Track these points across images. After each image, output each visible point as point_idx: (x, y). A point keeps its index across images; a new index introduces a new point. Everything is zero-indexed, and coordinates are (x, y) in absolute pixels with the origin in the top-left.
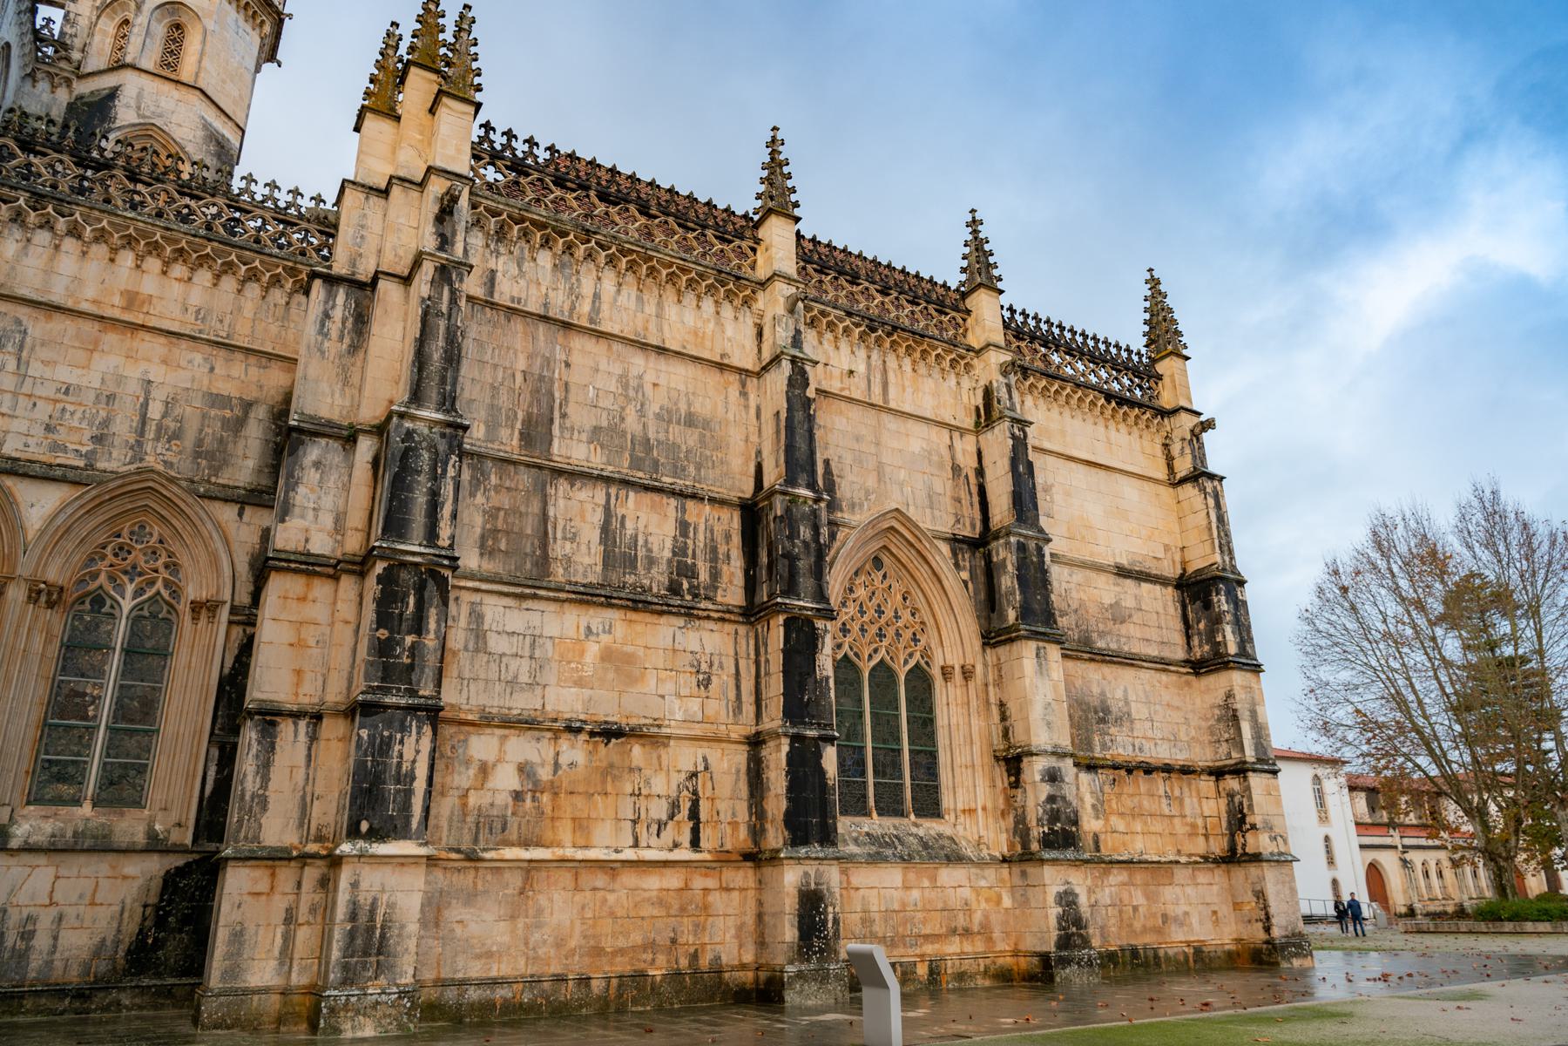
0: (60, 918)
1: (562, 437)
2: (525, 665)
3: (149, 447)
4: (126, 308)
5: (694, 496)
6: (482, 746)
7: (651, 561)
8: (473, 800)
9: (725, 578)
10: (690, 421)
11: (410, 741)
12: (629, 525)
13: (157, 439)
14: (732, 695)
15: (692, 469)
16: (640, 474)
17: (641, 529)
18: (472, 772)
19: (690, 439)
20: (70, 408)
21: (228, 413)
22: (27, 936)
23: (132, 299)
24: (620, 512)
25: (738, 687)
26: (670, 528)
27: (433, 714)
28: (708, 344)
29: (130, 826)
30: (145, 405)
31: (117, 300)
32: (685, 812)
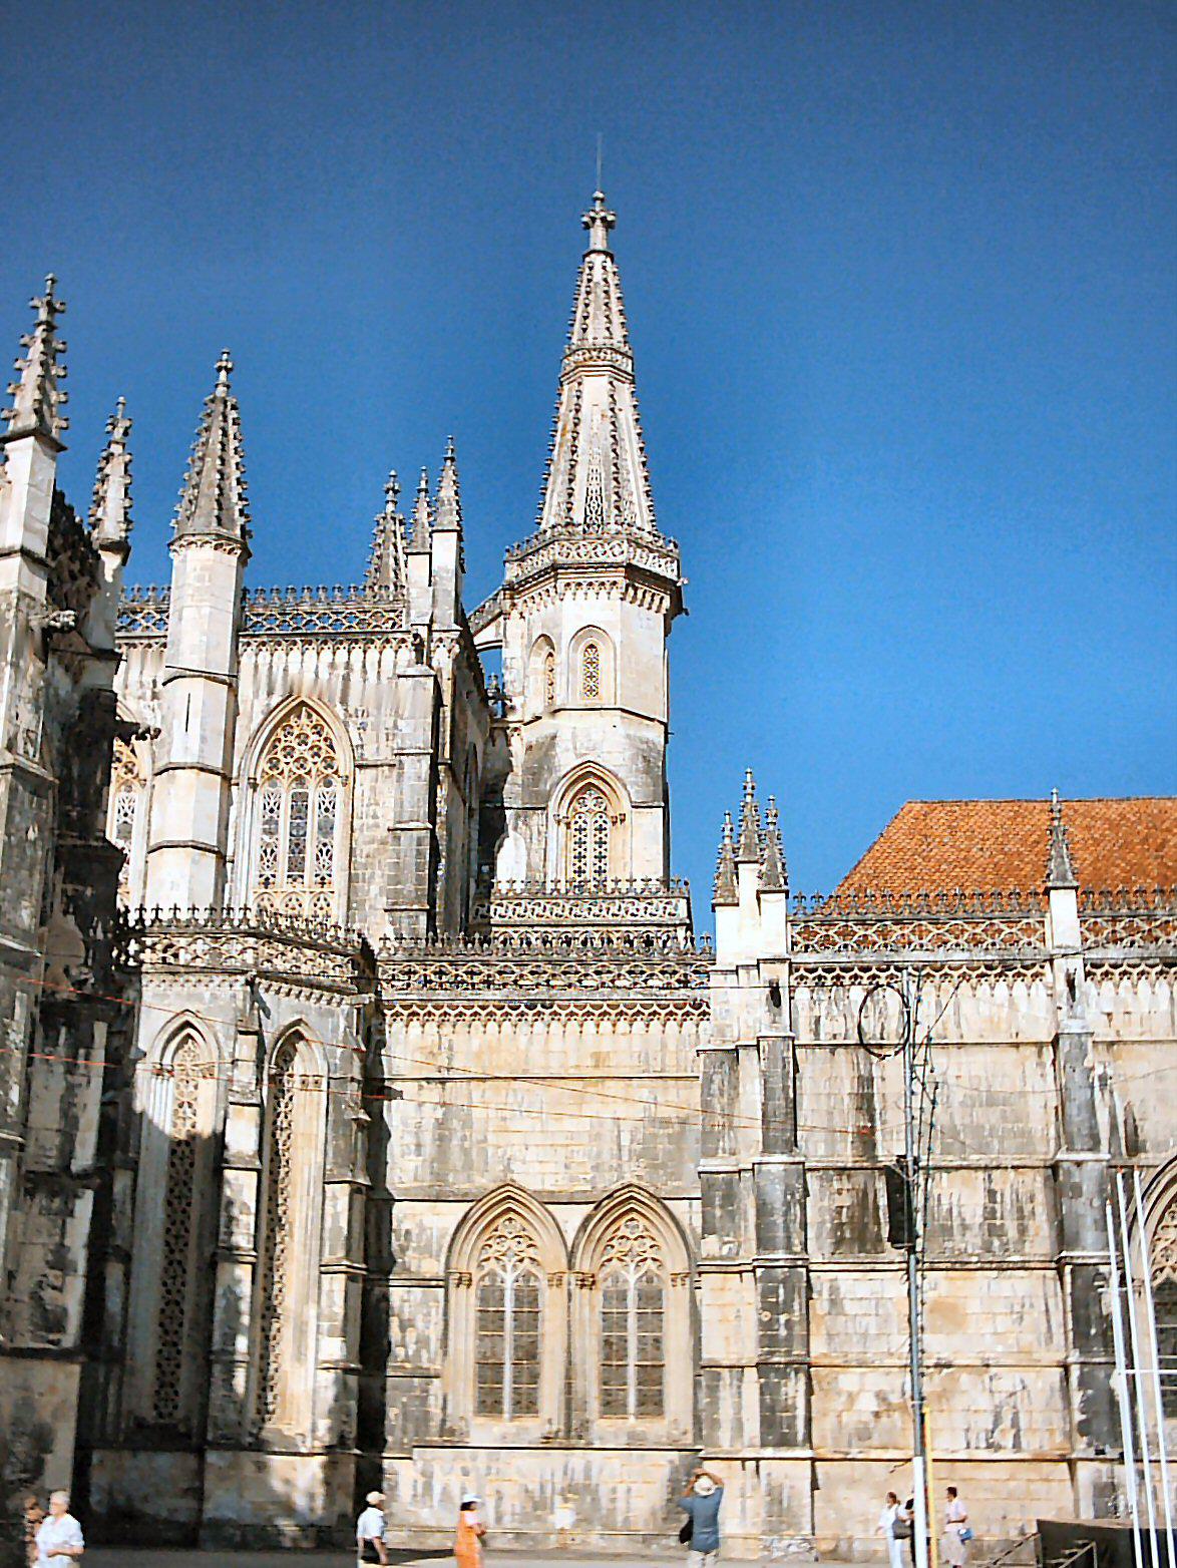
0: (629, 1490)
1: (884, 1140)
2: (872, 1320)
3: (625, 1168)
4: (596, 1066)
5: (998, 1168)
6: (848, 1381)
7: (965, 1227)
8: (845, 1417)
9: (1031, 1232)
10: (991, 1102)
11: (791, 1383)
12: (945, 1201)
13: (630, 1160)
14: (1044, 1328)
15: (996, 1145)
16: (950, 1158)
17: (955, 1202)
18: (843, 1398)
19: (991, 1117)
20: (576, 1148)
21: (670, 1131)
22: (613, 1500)
23: (598, 1059)
24: (936, 1192)
25: (1048, 1321)
26: (981, 1198)
27: (806, 1367)
28: (1004, 1026)
29: (655, 1429)
30: (619, 1136)
31: (590, 1062)
32: (1007, 1422)
